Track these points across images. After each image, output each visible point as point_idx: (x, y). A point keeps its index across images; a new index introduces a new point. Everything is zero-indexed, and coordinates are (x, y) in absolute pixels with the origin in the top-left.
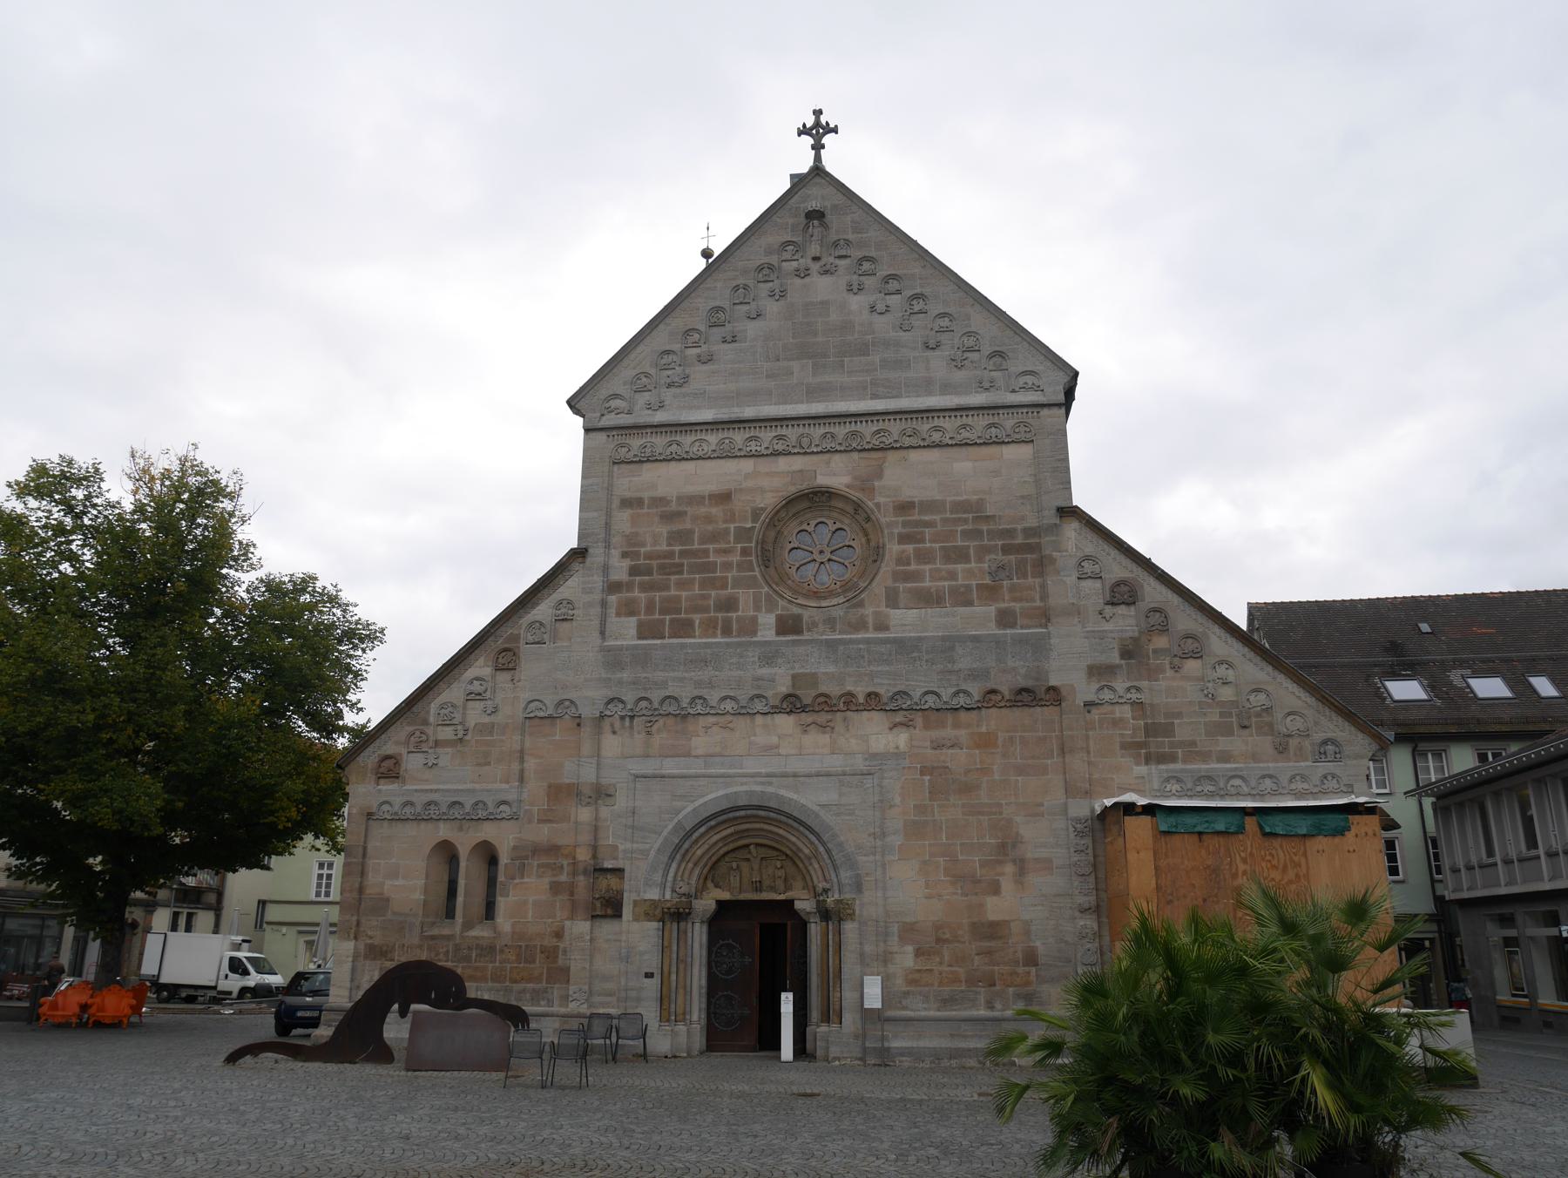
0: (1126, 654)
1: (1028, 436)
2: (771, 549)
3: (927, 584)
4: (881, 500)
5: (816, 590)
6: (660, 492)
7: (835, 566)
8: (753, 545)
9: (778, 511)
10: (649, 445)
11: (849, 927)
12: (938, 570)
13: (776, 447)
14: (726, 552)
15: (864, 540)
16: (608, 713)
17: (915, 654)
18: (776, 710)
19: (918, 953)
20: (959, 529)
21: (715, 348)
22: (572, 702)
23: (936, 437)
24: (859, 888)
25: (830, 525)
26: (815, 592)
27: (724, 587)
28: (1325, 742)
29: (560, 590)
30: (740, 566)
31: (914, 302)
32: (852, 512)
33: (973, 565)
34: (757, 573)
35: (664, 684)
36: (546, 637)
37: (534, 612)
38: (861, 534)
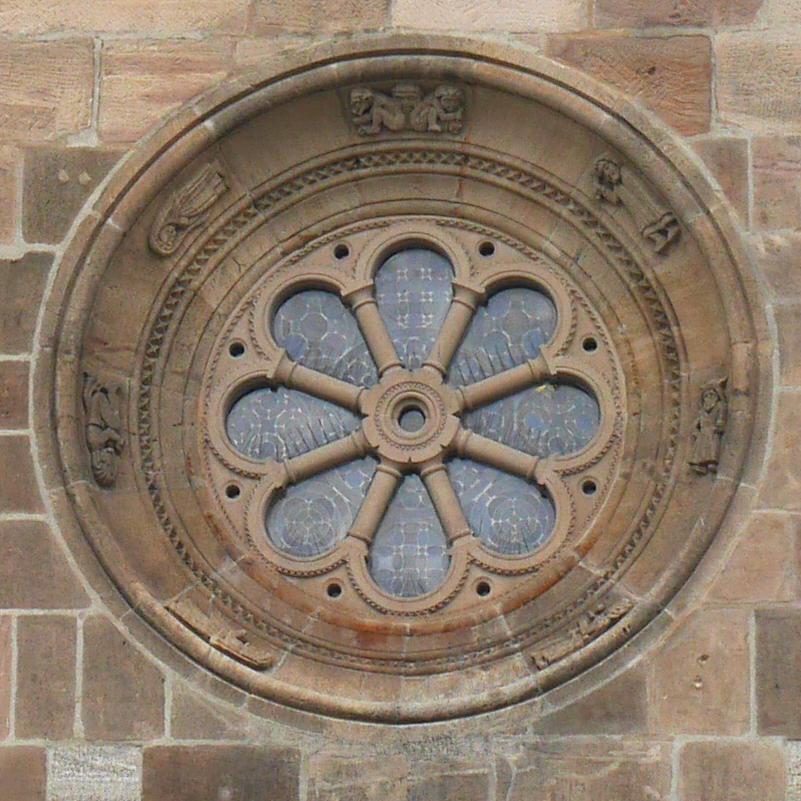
2: (132, 383)
4: (747, 129)
5: (371, 620)
7: (483, 489)
8: (31, 358)
9: (176, 177)
15: (645, 348)
25: (462, 265)
26: (367, 635)
32: (584, 188)
34: (49, 516)
38: (631, 319)
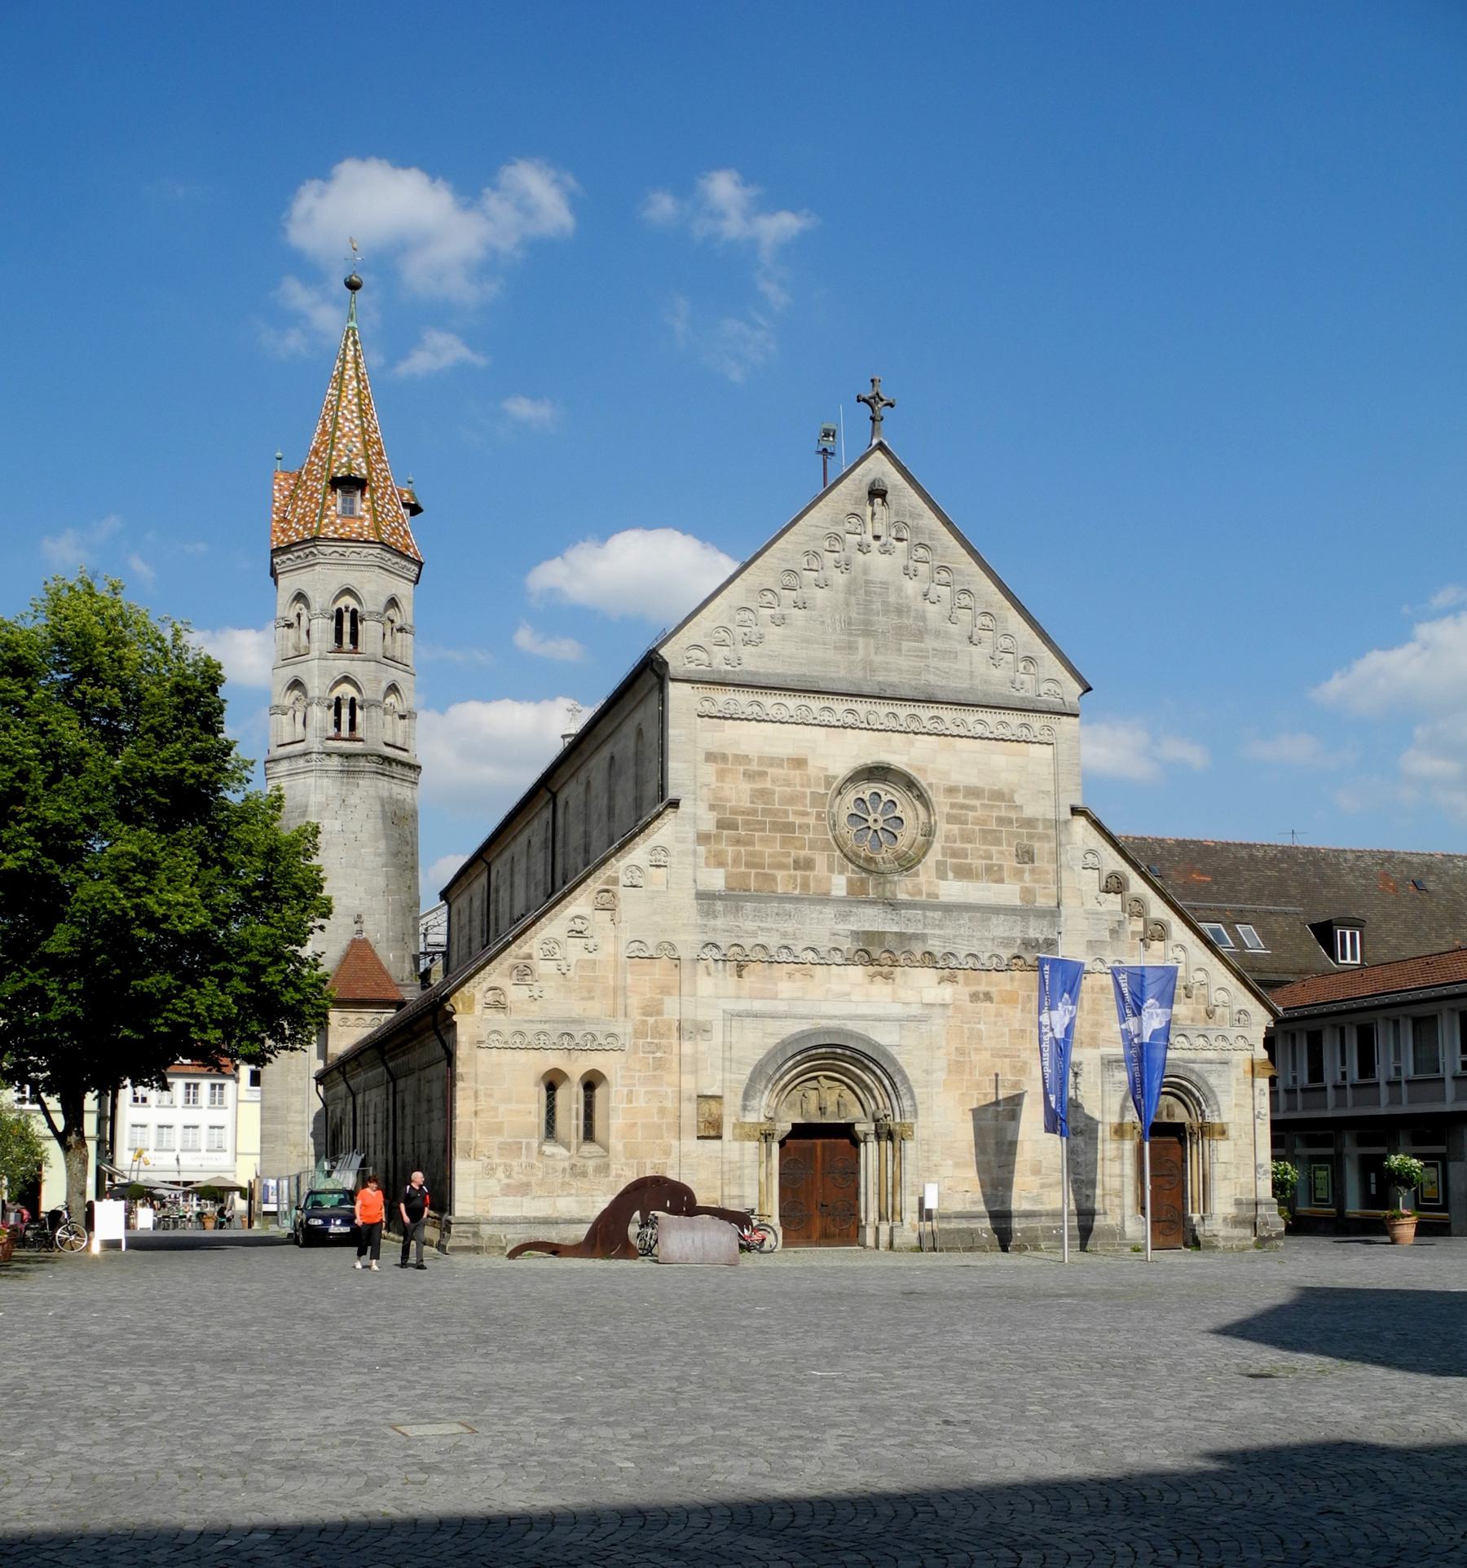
0: (1114, 932)
1: (1050, 738)
3: (968, 861)
4: (934, 781)
6: (743, 750)
10: (732, 702)
11: (909, 1146)
12: (978, 849)
13: (846, 720)
14: (805, 814)
16: (704, 956)
17: (961, 922)
18: (849, 962)
19: (956, 1165)
20: (995, 814)
21: (786, 612)
22: (671, 944)
23: (979, 729)
24: (915, 1114)
27: (802, 847)
28: (1240, 1012)
29: (654, 837)
30: (815, 828)
31: (961, 596)
33: (1004, 847)
35: (754, 934)
36: (641, 882)
37: (631, 856)
